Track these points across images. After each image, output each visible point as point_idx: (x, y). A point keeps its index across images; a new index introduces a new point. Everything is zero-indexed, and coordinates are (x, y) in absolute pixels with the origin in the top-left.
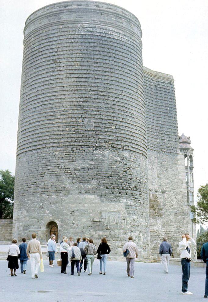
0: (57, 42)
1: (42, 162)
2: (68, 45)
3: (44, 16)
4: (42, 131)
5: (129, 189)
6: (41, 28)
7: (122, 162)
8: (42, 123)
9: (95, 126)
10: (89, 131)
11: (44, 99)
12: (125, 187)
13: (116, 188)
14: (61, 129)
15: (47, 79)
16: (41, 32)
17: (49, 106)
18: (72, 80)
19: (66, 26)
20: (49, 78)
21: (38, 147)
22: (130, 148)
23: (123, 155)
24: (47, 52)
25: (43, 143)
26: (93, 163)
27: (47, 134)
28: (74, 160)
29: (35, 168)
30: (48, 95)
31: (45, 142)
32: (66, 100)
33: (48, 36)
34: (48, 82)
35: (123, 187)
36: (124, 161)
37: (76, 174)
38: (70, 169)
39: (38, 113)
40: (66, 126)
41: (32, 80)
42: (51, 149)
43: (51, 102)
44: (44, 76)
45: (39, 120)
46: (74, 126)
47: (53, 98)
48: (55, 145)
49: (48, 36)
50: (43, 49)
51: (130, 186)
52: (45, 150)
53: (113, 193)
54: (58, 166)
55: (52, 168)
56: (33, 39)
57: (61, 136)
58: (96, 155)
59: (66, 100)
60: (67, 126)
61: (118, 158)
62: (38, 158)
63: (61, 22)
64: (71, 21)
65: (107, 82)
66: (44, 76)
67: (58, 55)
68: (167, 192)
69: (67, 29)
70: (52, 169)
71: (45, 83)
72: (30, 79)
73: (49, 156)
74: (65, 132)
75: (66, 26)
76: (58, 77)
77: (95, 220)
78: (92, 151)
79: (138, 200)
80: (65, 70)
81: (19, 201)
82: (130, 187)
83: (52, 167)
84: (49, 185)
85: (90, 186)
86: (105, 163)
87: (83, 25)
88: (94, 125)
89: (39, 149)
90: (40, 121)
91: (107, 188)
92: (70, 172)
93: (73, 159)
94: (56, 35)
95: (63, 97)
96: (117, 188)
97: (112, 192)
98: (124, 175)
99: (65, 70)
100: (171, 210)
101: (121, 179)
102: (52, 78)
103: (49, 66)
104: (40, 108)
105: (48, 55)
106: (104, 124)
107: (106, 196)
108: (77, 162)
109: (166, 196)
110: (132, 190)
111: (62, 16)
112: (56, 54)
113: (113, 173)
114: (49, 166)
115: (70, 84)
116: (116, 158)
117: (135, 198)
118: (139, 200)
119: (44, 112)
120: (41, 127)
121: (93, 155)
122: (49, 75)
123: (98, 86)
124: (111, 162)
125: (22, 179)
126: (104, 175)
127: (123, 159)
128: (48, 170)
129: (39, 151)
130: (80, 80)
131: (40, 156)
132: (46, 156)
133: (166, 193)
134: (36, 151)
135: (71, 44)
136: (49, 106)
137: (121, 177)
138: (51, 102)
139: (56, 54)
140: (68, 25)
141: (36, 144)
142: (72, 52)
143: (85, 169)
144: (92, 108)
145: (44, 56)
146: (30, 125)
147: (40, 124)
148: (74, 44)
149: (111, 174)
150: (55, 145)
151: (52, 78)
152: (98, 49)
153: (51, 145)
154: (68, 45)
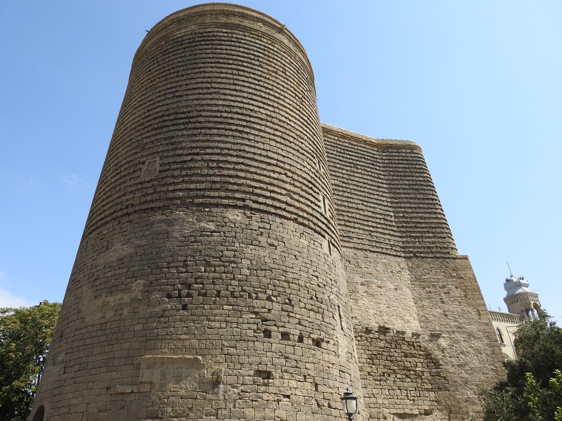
5: (241, 296)
7: (220, 232)
13: (195, 293)
22: (248, 203)
23: (224, 218)
26: (143, 242)
35: (219, 292)
36: (225, 229)
51: (244, 288)
53: (185, 307)
58: (153, 224)
68: (443, 335)
78: (146, 219)
79: (275, 325)
82: (243, 291)
85: (126, 298)
86: (171, 237)
96: (199, 295)
100: (464, 374)
107: (162, 316)
109: (443, 342)
116: (203, 224)
118: (279, 324)
127: (226, 225)
133: (444, 337)
137: (215, 266)
143: (125, 260)
149: (185, 261)
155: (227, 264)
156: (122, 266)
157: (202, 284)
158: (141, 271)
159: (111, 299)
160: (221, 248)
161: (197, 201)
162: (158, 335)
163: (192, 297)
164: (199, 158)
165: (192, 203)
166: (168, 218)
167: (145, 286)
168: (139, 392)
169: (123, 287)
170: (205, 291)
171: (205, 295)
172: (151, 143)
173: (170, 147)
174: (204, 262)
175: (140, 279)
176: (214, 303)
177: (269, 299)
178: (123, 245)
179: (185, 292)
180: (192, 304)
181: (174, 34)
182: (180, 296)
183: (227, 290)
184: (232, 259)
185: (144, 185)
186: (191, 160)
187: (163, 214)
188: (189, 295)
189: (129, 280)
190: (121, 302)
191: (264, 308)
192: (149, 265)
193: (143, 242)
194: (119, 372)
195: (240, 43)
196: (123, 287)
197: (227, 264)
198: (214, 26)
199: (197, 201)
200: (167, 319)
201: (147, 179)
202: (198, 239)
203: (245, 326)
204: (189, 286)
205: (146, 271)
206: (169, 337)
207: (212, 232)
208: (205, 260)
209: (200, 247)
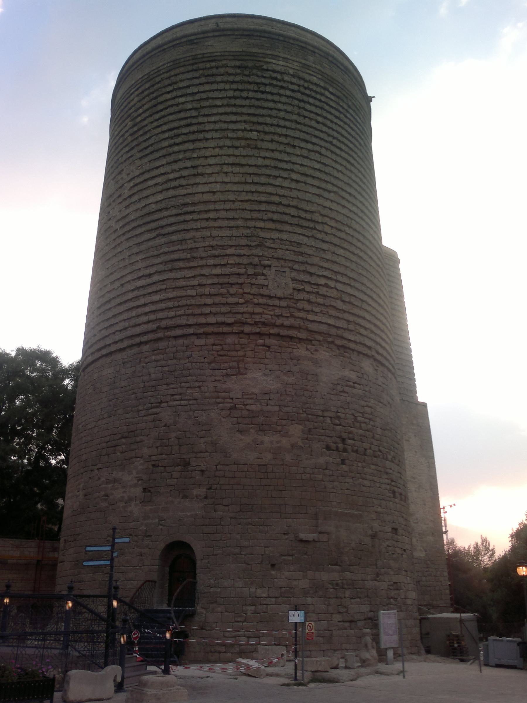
0: (197, 97)
1: (153, 376)
2: (225, 102)
3: (165, 47)
4: (156, 298)
6: (158, 71)
8: (156, 278)
9: (294, 289)
10: (280, 299)
11: (163, 223)
12: (370, 449)
13: (349, 448)
14: (207, 291)
15: (171, 176)
16: (157, 80)
17: (174, 238)
18: (237, 179)
19: (220, 64)
20: (177, 175)
21: (144, 339)
24: (171, 118)
25: (159, 328)
26: (291, 380)
27: (170, 304)
28: (242, 371)
29: (134, 393)
30: (174, 211)
31: (164, 323)
32: (220, 223)
33: (175, 86)
34: (176, 183)
35: (366, 449)
37: (248, 407)
38: (232, 395)
39: (147, 255)
40: (221, 284)
41: (132, 184)
42: (180, 341)
43: (181, 227)
44: (162, 170)
45: (148, 272)
46: (241, 284)
47: (188, 217)
48: (191, 331)
49: (175, 86)
50: (163, 113)
52: (162, 345)
53: (343, 462)
54: (196, 384)
55: (179, 390)
56: (136, 99)
57: (207, 310)
59: (220, 223)
60: (224, 286)
61: (351, 372)
62: (143, 367)
63: (208, 55)
64: (232, 54)
65: (318, 191)
66: (162, 170)
67: (200, 124)
69: (222, 70)
70: (180, 394)
71: (165, 186)
72: (126, 185)
73: (175, 361)
74: (218, 299)
75: (220, 64)
76: (200, 170)
77: (303, 536)
78: (289, 350)
80: (219, 155)
81: (81, 486)
82: (380, 451)
83: (181, 387)
84: (173, 435)
85: (285, 442)
87: (262, 64)
88: (291, 285)
89: (146, 343)
90: (150, 275)
91: (328, 448)
92: (231, 401)
93: (239, 368)
94: (196, 82)
95: (212, 215)
96: (353, 451)
97: (342, 460)
98: (365, 418)
99: (219, 155)
101: (360, 428)
102: (185, 173)
103: (176, 149)
104: (151, 243)
105: (176, 124)
106: (316, 287)
107: (326, 469)
108: (249, 375)
110: (383, 458)
111: (209, 43)
112: (194, 121)
113: (343, 411)
114: (172, 386)
115: (230, 187)
117: (392, 481)
119: (161, 251)
120: (154, 288)
121: (291, 359)
122: (176, 166)
123: (298, 198)
124: (336, 382)
125: (95, 426)
126: (320, 413)
128: (169, 398)
129: (145, 348)
130: (256, 179)
131: (147, 360)
132: (164, 360)
134: (136, 350)
135: (232, 102)
136: (174, 238)
137: (360, 423)
138: (181, 227)
139: (194, 121)
140: (225, 62)
141: (138, 330)
142: (234, 118)
144: (286, 245)
145: (165, 128)
146: (123, 287)
147: (149, 281)
148: (238, 102)
149: (337, 412)
150: (191, 331)
151: (185, 173)
152: (294, 117)
153: (178, 332)
154: (225, 102)
155: (367, 421)
156: (270, 402)
157: (353, 439)
158: (296, 414)
159: (266, 439)
160: (362, 403)
161: (338, 342)
162: (325, 488)
163: (348, 452)
164: (331, 284)
165: (333, 342)
166: (313, 356)
167: (303, 431)
168: (319, 541)
169: (279, 428)
170: (356, 448)
171: (356, 451)
172: (271, 241)
173: (301, 259)
174: (353, 417)
175: (297, 424)
176: (364, 461)
177: (392, 461)
178: (265, 375)
179: (341, 446)
180: (348, 459)
181: (269, 60)
182: (337, 449)
183: (370, 449)
184: (371, 416)
185: (277, 302)
186: (326, 285)
187: (307, 349)
188: (345, 450)
189: (284, 422)
190: (279, 445)
191: (391, 469)
192: (304, 410)
193: (291, 380)
194: (295, 520)
195: (346, 116)
196: (279, 428)
197: (367, 421)
198: (320, 76)
199: (338, 342)
200: (331, 472)
201: (279, 294)
202: (346, 389)
203: (384, 486)
204: (343, 440)
205: (302, 416)
206: (335, 491)
207: (354, 383)
208: (353, 414)
209: (348, 399)
